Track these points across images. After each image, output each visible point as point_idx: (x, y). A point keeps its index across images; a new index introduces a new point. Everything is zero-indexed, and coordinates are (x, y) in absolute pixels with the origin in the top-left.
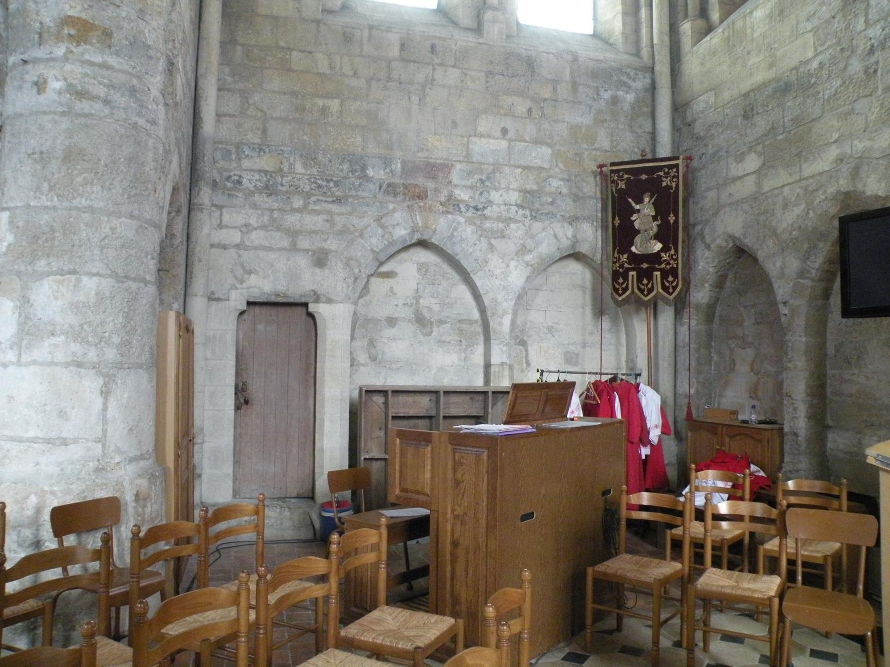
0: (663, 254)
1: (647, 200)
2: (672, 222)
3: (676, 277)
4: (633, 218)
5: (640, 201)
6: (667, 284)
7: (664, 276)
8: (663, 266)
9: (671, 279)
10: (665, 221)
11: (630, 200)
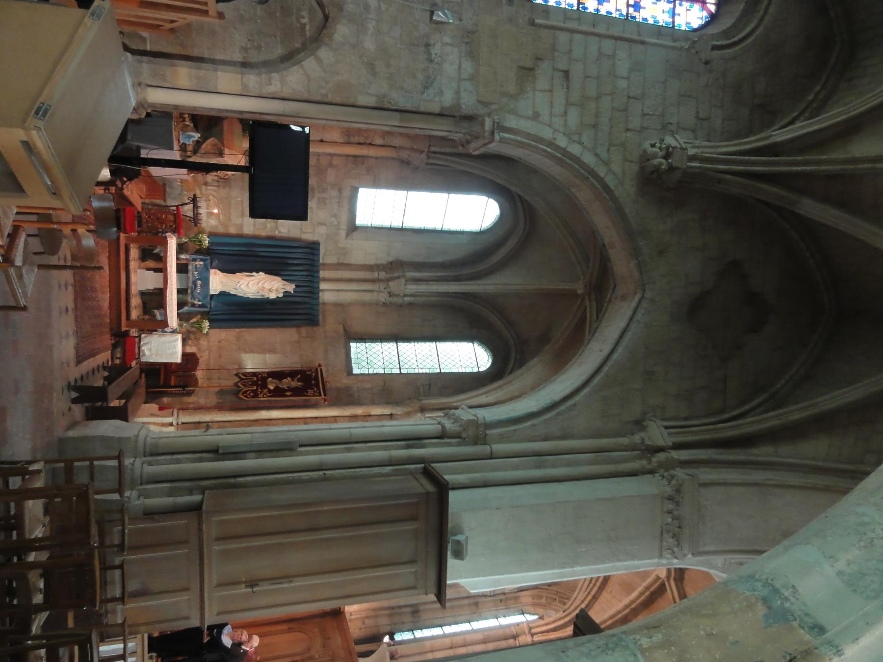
3: (253, 397)
5: (299, 381)
7: (253, 391)
10: (287, 391)
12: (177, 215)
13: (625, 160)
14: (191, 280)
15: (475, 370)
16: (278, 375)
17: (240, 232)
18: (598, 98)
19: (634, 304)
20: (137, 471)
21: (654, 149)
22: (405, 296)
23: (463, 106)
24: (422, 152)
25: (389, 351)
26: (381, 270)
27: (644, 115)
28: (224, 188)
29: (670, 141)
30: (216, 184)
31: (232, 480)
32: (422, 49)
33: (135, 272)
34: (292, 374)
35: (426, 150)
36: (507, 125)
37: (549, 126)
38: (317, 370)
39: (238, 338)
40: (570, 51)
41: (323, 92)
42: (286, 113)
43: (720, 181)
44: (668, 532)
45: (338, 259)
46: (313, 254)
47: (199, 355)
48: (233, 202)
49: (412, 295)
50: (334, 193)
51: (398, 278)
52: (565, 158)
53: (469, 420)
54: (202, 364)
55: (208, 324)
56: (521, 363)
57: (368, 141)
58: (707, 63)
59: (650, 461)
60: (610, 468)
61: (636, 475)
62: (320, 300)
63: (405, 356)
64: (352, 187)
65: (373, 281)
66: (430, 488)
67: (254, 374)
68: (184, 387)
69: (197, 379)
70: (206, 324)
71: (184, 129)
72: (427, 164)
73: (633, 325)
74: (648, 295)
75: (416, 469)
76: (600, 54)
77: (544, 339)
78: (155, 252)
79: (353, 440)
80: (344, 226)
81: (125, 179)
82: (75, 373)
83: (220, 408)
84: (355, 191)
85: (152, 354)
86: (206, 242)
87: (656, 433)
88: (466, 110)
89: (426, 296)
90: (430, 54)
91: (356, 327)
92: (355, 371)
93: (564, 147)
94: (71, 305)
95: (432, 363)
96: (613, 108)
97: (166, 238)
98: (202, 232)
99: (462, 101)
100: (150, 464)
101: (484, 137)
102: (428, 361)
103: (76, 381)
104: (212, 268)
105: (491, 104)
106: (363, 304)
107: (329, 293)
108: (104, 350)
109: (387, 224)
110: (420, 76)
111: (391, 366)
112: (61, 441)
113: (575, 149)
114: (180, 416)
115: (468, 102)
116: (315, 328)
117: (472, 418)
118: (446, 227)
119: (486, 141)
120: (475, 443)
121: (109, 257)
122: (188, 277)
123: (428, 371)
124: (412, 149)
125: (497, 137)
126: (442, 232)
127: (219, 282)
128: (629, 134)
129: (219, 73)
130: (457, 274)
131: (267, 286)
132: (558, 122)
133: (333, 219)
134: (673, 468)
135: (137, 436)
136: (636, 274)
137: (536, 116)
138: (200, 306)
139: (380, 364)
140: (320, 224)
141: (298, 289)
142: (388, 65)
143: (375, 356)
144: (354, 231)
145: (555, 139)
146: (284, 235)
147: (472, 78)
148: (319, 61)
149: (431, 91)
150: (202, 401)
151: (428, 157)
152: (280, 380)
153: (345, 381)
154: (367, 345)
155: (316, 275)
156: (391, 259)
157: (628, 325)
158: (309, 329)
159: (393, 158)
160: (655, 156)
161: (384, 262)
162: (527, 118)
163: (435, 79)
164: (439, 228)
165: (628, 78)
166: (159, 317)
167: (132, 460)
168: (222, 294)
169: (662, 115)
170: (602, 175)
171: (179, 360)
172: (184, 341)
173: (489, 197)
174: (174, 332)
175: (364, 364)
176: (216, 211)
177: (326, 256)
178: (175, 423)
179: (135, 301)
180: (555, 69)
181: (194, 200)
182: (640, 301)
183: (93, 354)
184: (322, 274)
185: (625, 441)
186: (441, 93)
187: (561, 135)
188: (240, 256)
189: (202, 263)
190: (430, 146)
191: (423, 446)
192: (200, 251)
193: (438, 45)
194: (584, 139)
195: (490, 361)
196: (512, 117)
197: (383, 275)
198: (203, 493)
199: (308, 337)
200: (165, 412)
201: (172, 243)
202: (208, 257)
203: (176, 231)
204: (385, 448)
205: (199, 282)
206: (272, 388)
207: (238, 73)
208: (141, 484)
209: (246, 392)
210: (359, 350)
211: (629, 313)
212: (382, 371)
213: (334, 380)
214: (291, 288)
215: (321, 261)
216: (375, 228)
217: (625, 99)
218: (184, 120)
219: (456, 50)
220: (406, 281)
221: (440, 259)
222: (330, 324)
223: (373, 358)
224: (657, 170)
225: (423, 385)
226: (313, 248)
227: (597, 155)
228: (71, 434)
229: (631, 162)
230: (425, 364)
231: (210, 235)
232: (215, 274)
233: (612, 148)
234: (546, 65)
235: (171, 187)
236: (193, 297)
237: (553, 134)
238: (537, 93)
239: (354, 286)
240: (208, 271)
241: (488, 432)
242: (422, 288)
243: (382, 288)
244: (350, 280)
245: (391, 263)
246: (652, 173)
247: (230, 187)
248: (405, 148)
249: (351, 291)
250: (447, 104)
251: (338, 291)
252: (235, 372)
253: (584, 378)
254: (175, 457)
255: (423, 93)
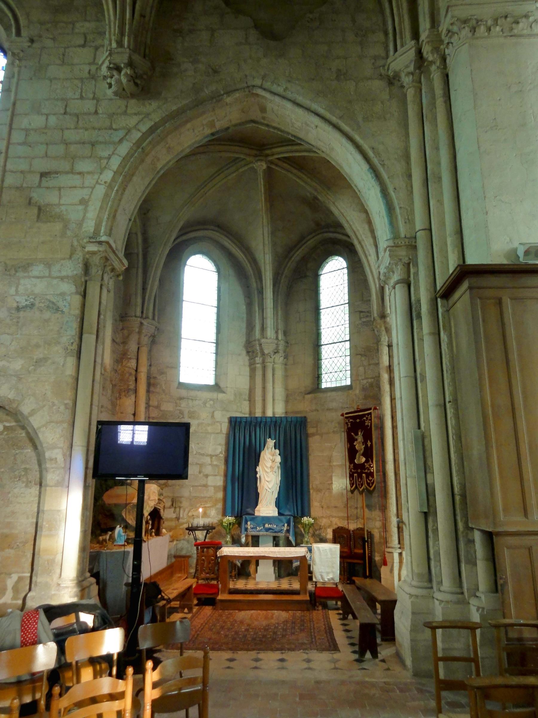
0: (366, 464)
1: (360, 433)
2: (369, 445)
3: (373, 477)
4: (355, 444)
6: (369, 482)
7: (367, 477)
8: (366, 471)
9: (370, 478)
10: (367, 445)
11: (352, 434)
12: (202, 546)
13: (125, 113)
14: (265, 533)
15: (346, 271)
16: (352, 453)
17: (222, 489)
18: (67, 144)
19: (268, 95)
20: (448, 597)
21: (113, 83)
22: (277, 338)
23: (75, 272)
24: (141, 323)
25: (329, 352)
26: (255, 361)
27: (82, 98)
28: (181, 502)
29: (104, 70)
30: (178, 509)
31: (457, 498)
32: (22, 314)
33: (257, 583)
34: (351, 440)
35: (139, 319)
36: (92, 230)
37: (93, 188)
38: (346, 418)
39: (319, 490)
40: (22, 172)
41: (62, 408)
42: (85, 444)
43: (142, 16)
44: (511, 29)
45: (245, 400)
46: (240, 422)
47: (335, 527)
48: (194, 495)
49: (277, 332)
50: (183, 404)
51: (260, 345)
52: (126, 175)
53: (390, 256)
54: (343, 524)
55: (305, 518)
56: (338, 226)
57: (134, 372)
58: (32, 41)
59: (432, 63)
60: (440, 102)
61: (447, 76)
62: (283, 416)
63: (333, 337)
64: (178, 388)
65: (264, 368)
66: (465, 285)
67: (351, 476)
68: (364, 541)
69: (357, 529)
70: (305, 520)
71: (112, 538)
72: (153, 319)
73: (289, 95)
74: (258, 82)
75: (443, 306)
76: (24, 143)
77: (314, 204)
78: (239, 564)
79: (412, 374)
80: (214, 395)
81: (160, 596)
82: (346, 654)
83: (384, 508)
84: (182, 385)
85: (333, 572)
86: (231, 519)
87: (402, 60)
88: (79, 270)
89: (277, 319)
90: (26, 306)
91: (308, 382)
92: (348, 383)
93: (113, 173)
94: (277, 655)
95: (340, 312)
96: (76, 128)
97: (222, 557)
98: (221, 523)
99: (70, 274)
100: (441, 583)
101: (106, 251)
102: (338, 316)
103: (354, 652)
104: (254, 515)
105: (72, 246)
106: (286, 377)
107: (276, 408)
108: (327, 619)
109: (213, 356)
110: (47, 315)
111: (343, 349)
112: (416, 674)
113: (115, 162)
114: (393, 546)
115: (72, 268)
116: (309, 420)
117: (388, 253)
118: (215, 304)
119: (109, 250)
120: (415, 248)
121: (240, 610)
122: (263, 535)
123: (348, 315)
124: (140, 333)
125: (104, 238)
126: (218, 307)
127: (267, 508)
128: (100, 111)
129: (45, 509)
130: (256, 292)
131: (269, 464)
132: (89, 181)
133: (208, 405)
134: (439, 35)
135: (411, 596)
136: (237, 95)
137: (84, 202)
138: (289, 525)
139: (341, 360)
140: (213, 416)
141: (273, 436)
142: (37, 346)
143: (333, 365)
144: (219, 387)
145: (105, 182)
146: (224, 449)
147: (49, 265)
148: (33, 413)
149: (61, 304)
150: (378, 524)
151: (147, 318)
152: (356, 451)
153: (357, 392)
154: (323, 372)
155: (259, 420)
156: (244, 352)
157: (289, 100)
158: (309, 425)
159: (150, 351)
160: (119, 82)
161: (247, 358)
162: (85, 211)
163: (50, 301)
164: (215, 310)
165: (47, 115)
166: (298, 563)
167: (437, 603)
168: (278, 504)
169: (82, 80)
170: (139, 135)
171: (337, 547)
172: (323, 540)
173: (185, 264)
174: (310, 550)
175: (341, 375)
176: (201, 510)
177: (242, 411)
178: (399, 551)
179: (285, 584)
180: (39, 186)
181: (192, 529)
182: (265, 89)
183: (330, 631)
184: (258, 414)
185: (410, 93)
186: (63, 294)
187: (102, 177)
188: (242, 488)
189: (249, 523)
190: (136, 316)
191: (419, 301)
192: (240, 524)
193: (18, 298)
194: (105, 154)
195: (337, 258)
196: (85, 225)
197: (258, 360)
198: (472, 529)
199: (317, 427)
200: (388, 560)
201: (228, 551)
202: (244, 517)
203: (218, 546)
204: (421, 340)
205: (267, 526)
206: (364, 460)
207: (46, 490)
208: (462, 593)
209: (368, 484)
210: (329, 380)
211: (277, 99)
212: (348, 358)
213: (355, 402)
214: (271, 443)
215: (247, 416)
216: (216, 367)
217: (67, 117)
218: (105, 540)
219: (22, 281)
220: (264, 338)
221: (244, 308)
222: (304, 407)
223: (336, 367)
224: (133, 79)
225: (360, 318)
226: (235, 423)
227: (121, 141)
228: (409, 662)
229: (127, 106)
230: (340, 319)
231: (224, 514)
232: (259, 511)
233: (114, 126)
234: (35, 195)
235: (182, 549)
236: (281, 531)
237: (100, 184)
238: (62, 202)
239: (269, 386)
240: (257, 517)
241: (403, 235)
242: (270, 322)
243: (272, 360)
244: (264, 388)
245: (248, 352)
246: (136, 84)
247: (181, 497)
248: (139, 338)
249: (273, 388)
250: (73, 289)
251: (274, 400)
252: (350, 493)
253: (344, 140)
254: (432, 556)
255: (63, 312)
